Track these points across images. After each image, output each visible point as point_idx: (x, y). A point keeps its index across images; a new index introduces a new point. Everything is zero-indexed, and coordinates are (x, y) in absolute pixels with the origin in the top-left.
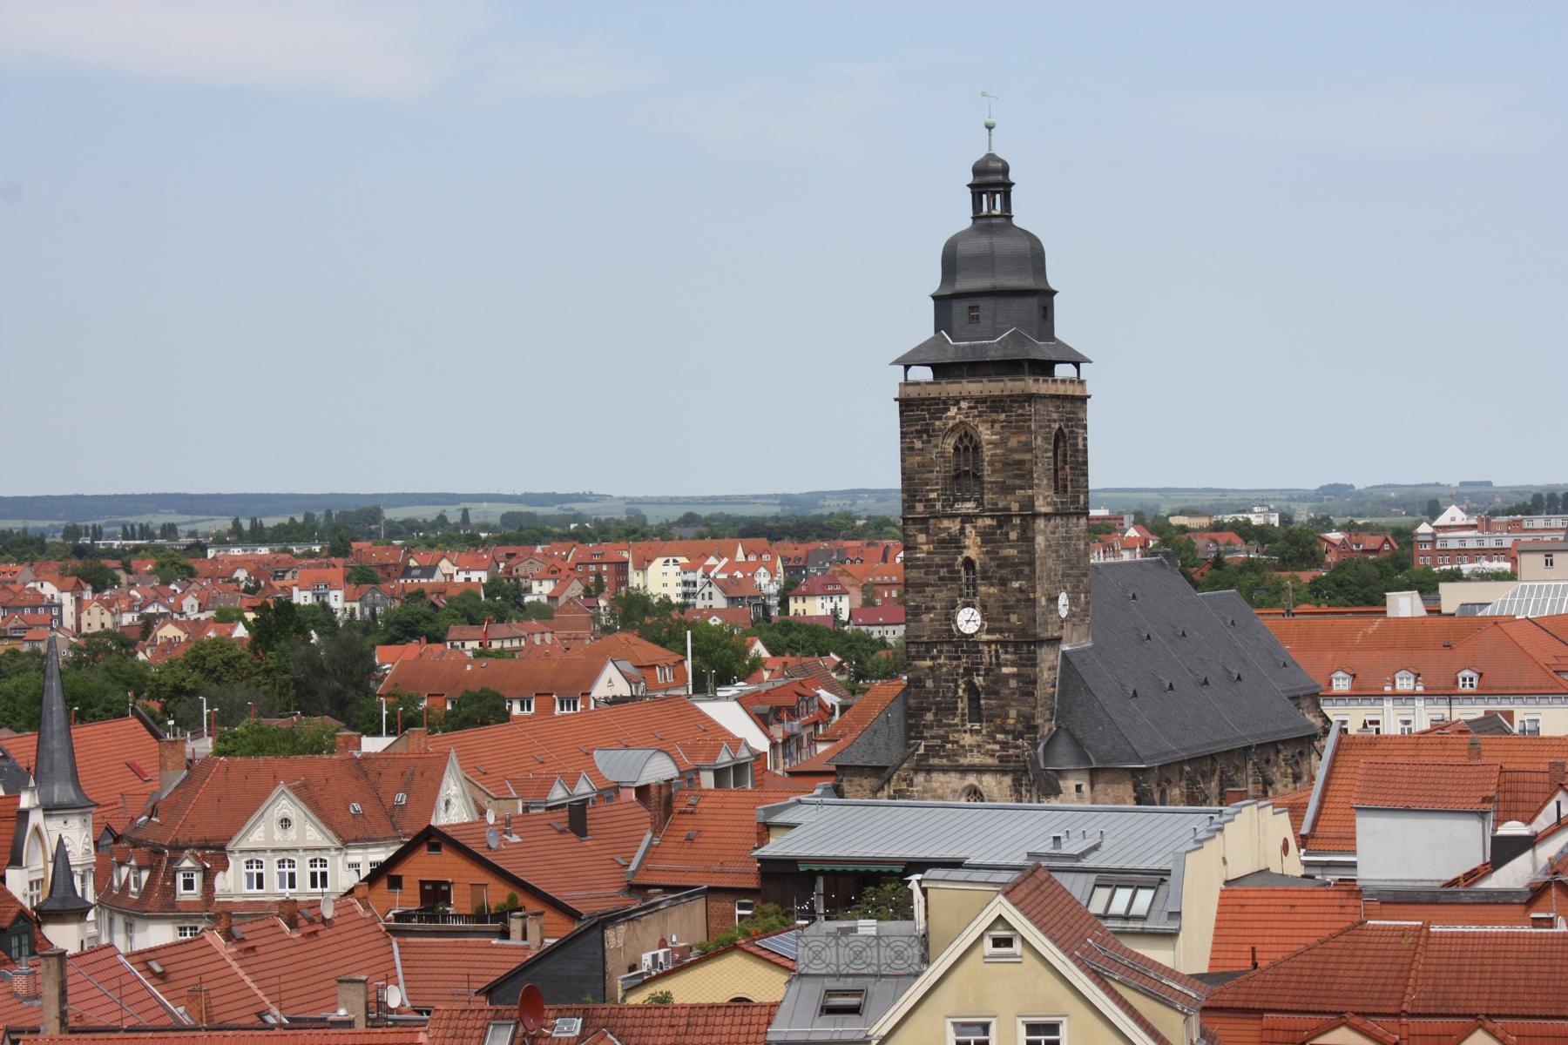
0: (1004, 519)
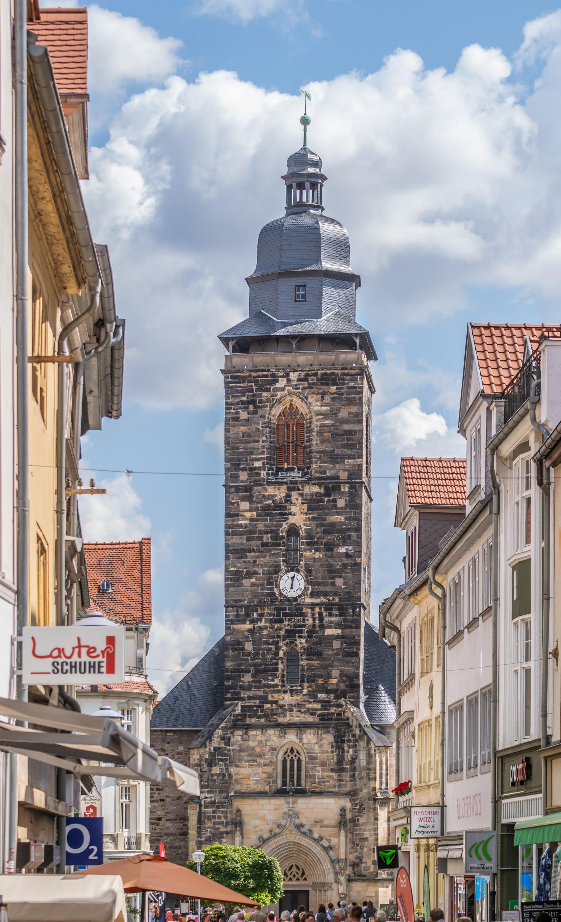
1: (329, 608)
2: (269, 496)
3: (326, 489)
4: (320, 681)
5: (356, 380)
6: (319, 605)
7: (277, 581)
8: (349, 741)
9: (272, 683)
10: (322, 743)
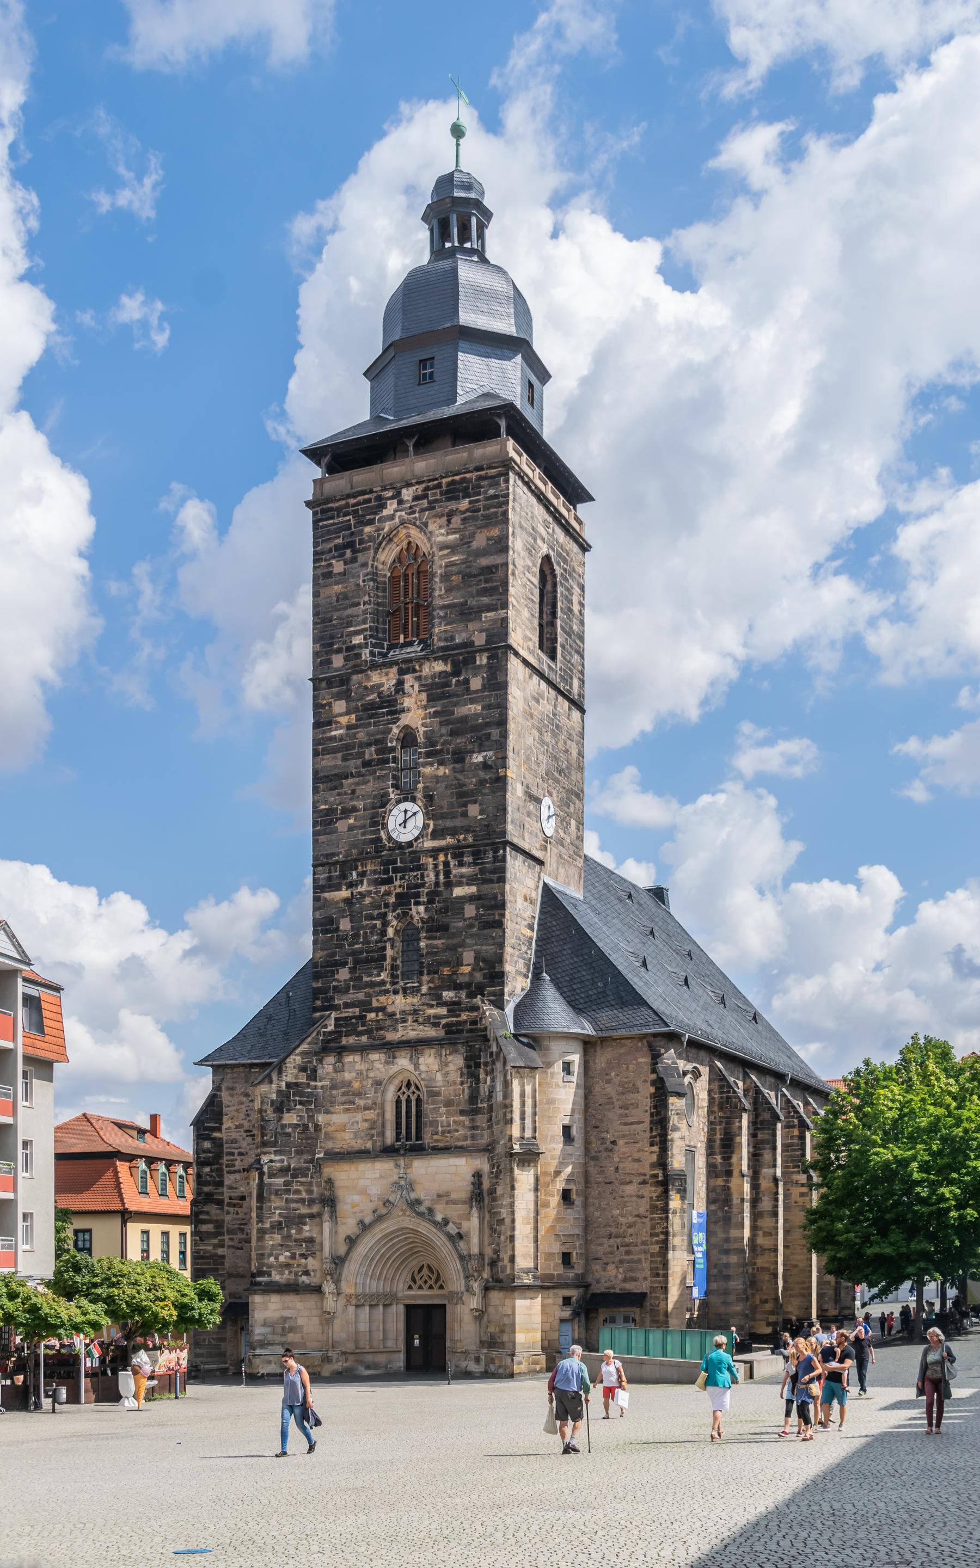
0: (461, 657)
1: (458, 852)
2: (373, 686)
3: (455, 664)
4: (446, 971)
5: (498, 484)
7: (384, 817)
8: (486, 1064)
9: (378, 979)
10: (447, 1069)
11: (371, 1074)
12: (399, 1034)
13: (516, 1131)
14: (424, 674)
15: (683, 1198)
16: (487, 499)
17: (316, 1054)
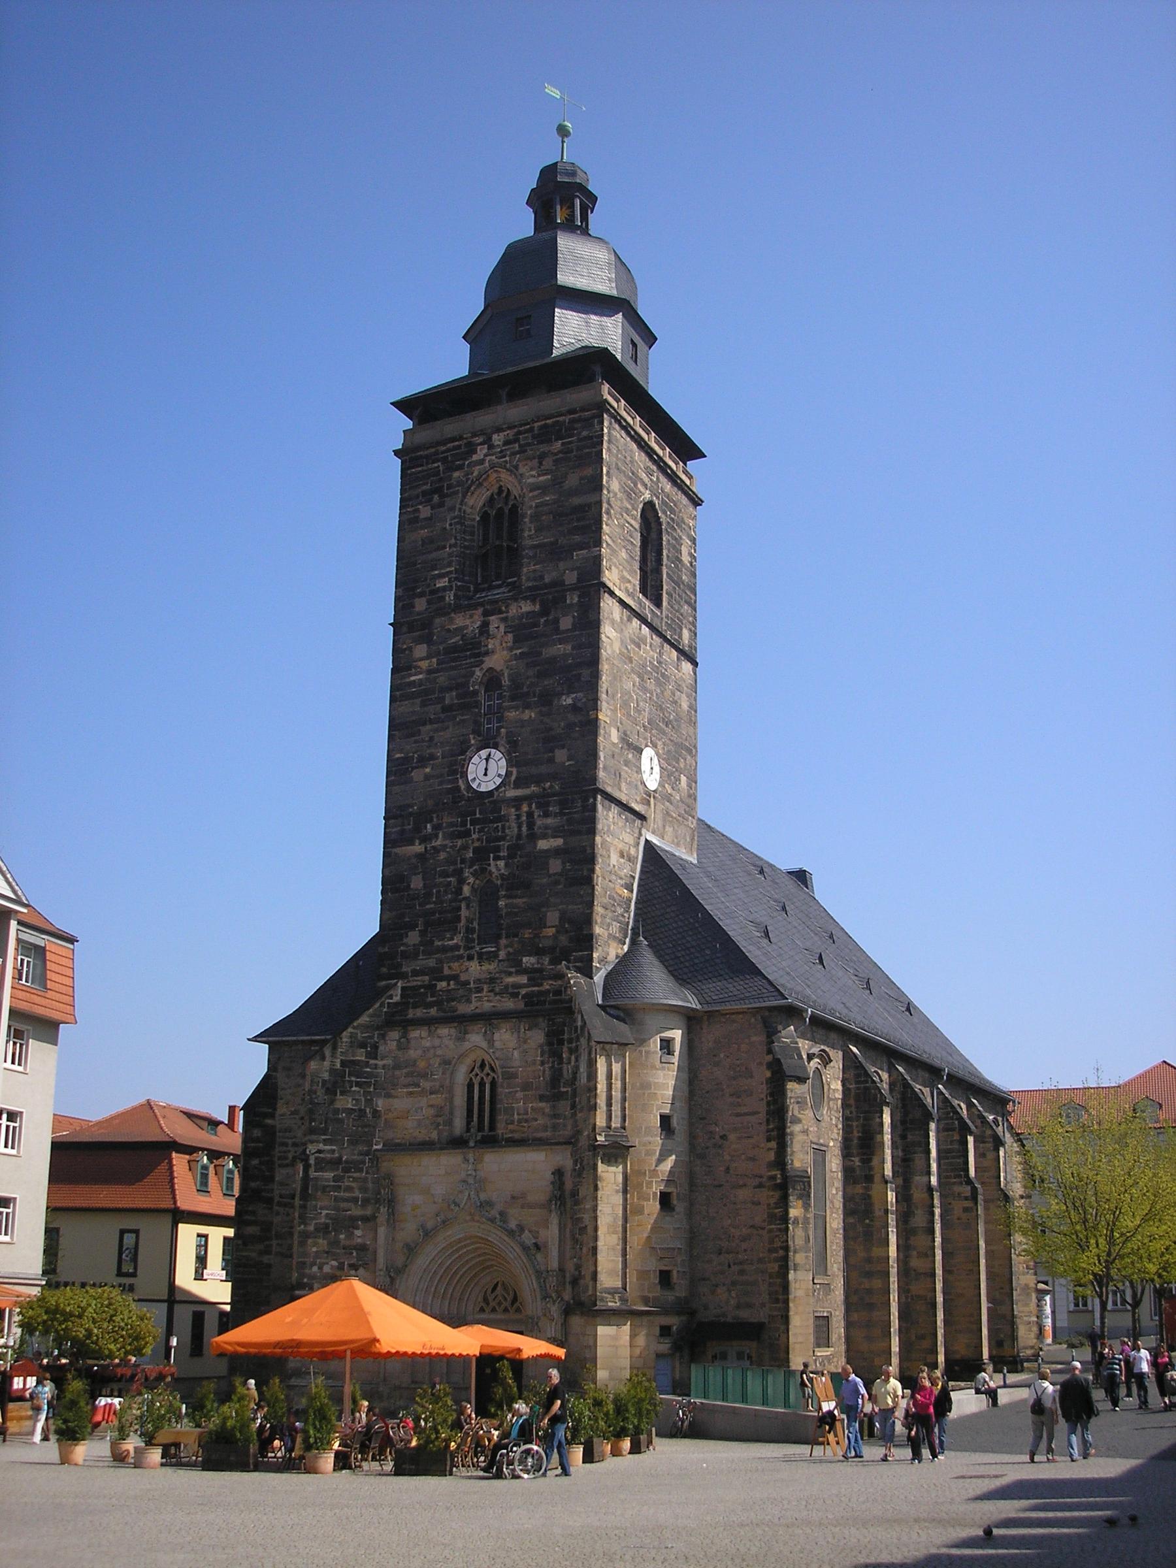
0: (550, 598)
1: (542, 801)
2: (456, 629)
4: (527, 934)
5: (592, 425)
6: (528, 798)
8: (570, 1041)
11: (439, 1052)
12: (472, 1007)
13: (600, 1120)
14: (510, 614)
15: (806, 1206)
16: (580, 440)
17: (378, 1028)
